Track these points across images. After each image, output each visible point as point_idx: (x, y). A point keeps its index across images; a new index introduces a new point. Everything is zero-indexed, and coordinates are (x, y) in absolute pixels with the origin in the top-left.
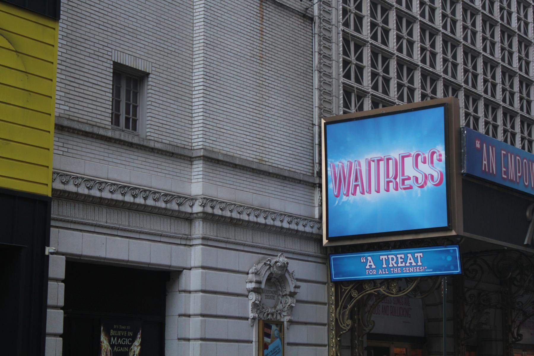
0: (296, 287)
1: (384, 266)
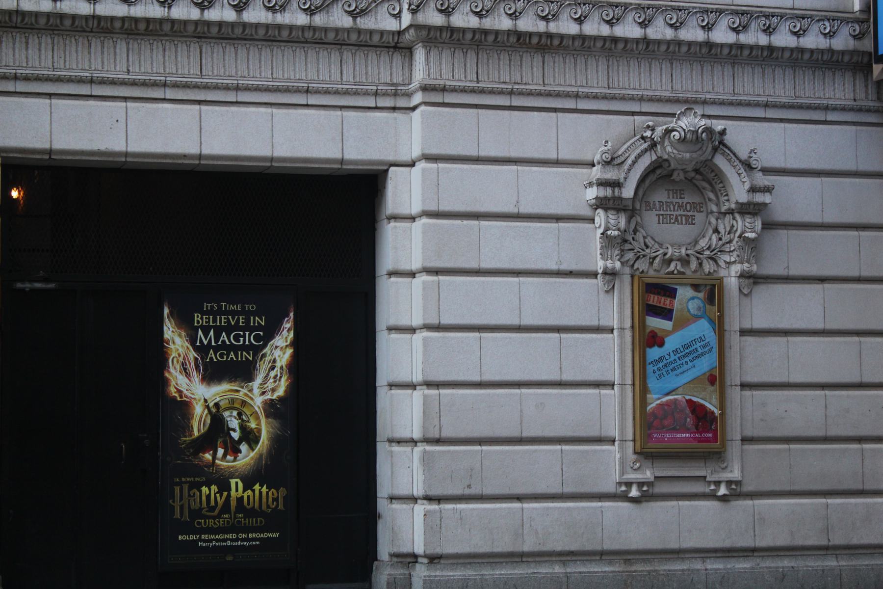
0: (753, 190)
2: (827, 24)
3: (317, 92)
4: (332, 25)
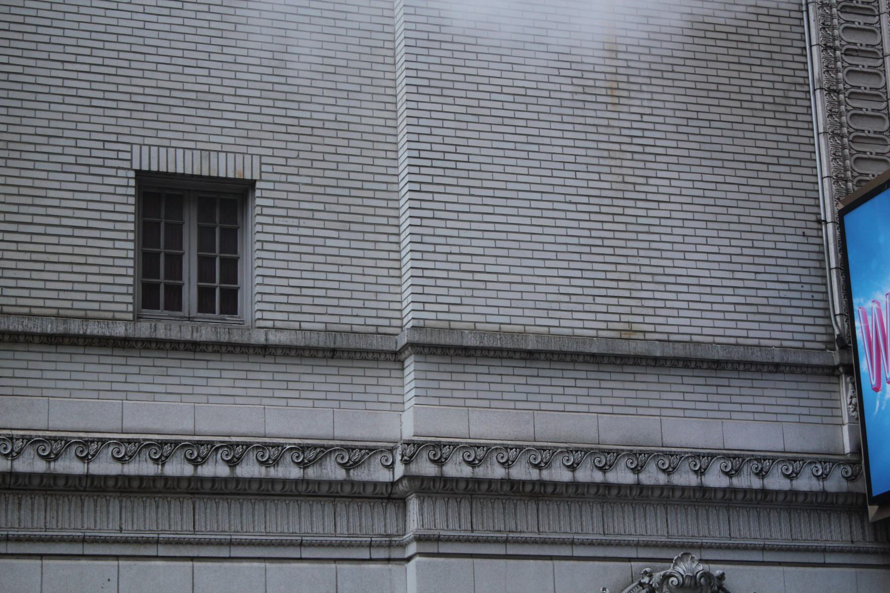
2: (819, 466)
3: (311, 545)
4: (325, 478)
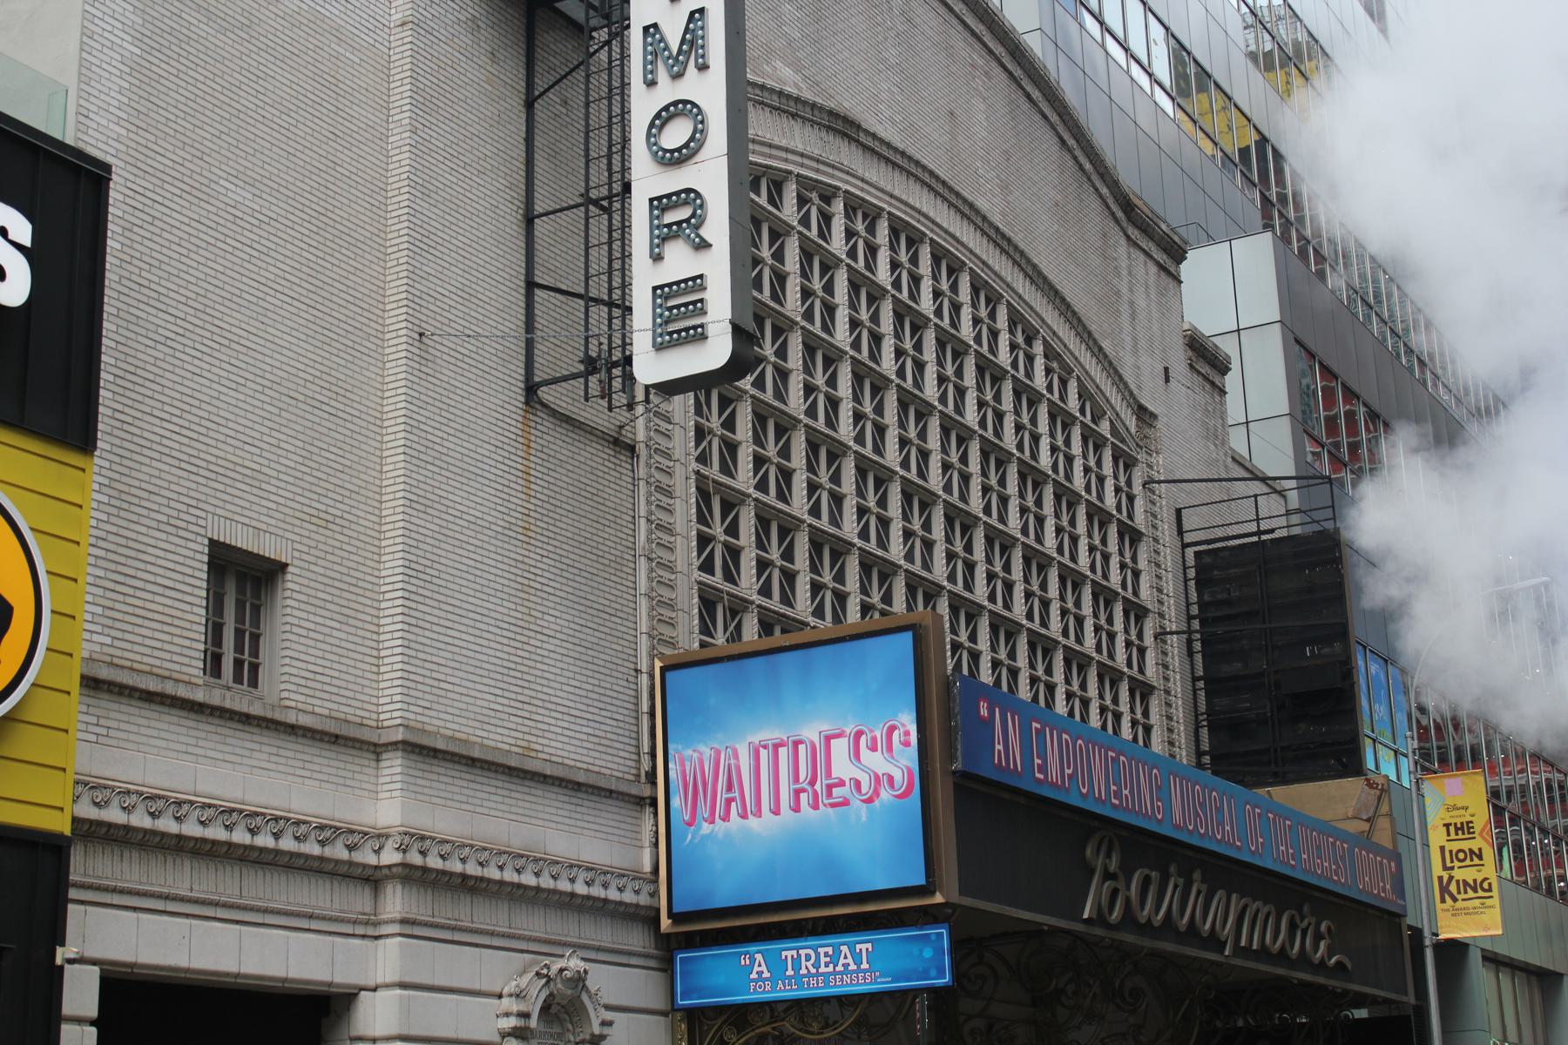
1: (790, 972)
